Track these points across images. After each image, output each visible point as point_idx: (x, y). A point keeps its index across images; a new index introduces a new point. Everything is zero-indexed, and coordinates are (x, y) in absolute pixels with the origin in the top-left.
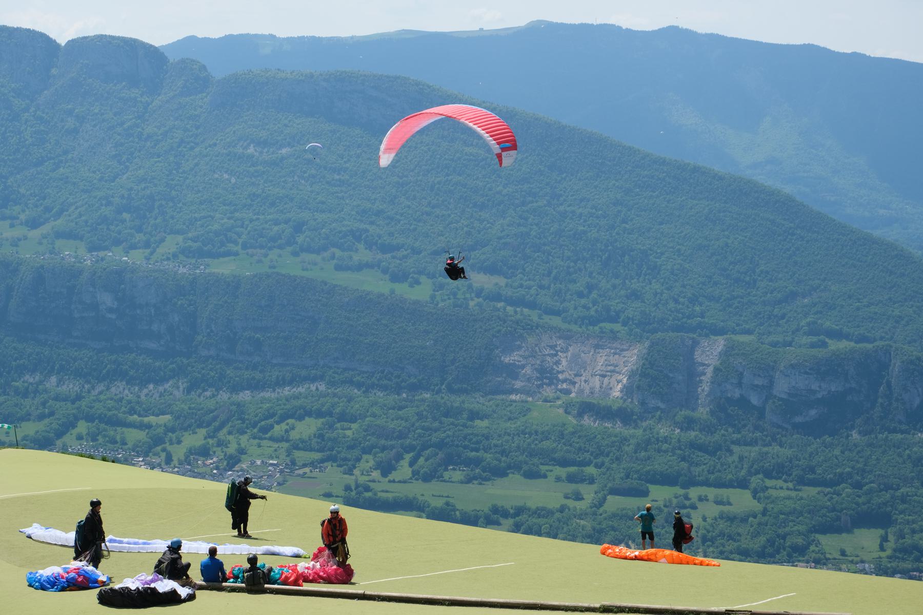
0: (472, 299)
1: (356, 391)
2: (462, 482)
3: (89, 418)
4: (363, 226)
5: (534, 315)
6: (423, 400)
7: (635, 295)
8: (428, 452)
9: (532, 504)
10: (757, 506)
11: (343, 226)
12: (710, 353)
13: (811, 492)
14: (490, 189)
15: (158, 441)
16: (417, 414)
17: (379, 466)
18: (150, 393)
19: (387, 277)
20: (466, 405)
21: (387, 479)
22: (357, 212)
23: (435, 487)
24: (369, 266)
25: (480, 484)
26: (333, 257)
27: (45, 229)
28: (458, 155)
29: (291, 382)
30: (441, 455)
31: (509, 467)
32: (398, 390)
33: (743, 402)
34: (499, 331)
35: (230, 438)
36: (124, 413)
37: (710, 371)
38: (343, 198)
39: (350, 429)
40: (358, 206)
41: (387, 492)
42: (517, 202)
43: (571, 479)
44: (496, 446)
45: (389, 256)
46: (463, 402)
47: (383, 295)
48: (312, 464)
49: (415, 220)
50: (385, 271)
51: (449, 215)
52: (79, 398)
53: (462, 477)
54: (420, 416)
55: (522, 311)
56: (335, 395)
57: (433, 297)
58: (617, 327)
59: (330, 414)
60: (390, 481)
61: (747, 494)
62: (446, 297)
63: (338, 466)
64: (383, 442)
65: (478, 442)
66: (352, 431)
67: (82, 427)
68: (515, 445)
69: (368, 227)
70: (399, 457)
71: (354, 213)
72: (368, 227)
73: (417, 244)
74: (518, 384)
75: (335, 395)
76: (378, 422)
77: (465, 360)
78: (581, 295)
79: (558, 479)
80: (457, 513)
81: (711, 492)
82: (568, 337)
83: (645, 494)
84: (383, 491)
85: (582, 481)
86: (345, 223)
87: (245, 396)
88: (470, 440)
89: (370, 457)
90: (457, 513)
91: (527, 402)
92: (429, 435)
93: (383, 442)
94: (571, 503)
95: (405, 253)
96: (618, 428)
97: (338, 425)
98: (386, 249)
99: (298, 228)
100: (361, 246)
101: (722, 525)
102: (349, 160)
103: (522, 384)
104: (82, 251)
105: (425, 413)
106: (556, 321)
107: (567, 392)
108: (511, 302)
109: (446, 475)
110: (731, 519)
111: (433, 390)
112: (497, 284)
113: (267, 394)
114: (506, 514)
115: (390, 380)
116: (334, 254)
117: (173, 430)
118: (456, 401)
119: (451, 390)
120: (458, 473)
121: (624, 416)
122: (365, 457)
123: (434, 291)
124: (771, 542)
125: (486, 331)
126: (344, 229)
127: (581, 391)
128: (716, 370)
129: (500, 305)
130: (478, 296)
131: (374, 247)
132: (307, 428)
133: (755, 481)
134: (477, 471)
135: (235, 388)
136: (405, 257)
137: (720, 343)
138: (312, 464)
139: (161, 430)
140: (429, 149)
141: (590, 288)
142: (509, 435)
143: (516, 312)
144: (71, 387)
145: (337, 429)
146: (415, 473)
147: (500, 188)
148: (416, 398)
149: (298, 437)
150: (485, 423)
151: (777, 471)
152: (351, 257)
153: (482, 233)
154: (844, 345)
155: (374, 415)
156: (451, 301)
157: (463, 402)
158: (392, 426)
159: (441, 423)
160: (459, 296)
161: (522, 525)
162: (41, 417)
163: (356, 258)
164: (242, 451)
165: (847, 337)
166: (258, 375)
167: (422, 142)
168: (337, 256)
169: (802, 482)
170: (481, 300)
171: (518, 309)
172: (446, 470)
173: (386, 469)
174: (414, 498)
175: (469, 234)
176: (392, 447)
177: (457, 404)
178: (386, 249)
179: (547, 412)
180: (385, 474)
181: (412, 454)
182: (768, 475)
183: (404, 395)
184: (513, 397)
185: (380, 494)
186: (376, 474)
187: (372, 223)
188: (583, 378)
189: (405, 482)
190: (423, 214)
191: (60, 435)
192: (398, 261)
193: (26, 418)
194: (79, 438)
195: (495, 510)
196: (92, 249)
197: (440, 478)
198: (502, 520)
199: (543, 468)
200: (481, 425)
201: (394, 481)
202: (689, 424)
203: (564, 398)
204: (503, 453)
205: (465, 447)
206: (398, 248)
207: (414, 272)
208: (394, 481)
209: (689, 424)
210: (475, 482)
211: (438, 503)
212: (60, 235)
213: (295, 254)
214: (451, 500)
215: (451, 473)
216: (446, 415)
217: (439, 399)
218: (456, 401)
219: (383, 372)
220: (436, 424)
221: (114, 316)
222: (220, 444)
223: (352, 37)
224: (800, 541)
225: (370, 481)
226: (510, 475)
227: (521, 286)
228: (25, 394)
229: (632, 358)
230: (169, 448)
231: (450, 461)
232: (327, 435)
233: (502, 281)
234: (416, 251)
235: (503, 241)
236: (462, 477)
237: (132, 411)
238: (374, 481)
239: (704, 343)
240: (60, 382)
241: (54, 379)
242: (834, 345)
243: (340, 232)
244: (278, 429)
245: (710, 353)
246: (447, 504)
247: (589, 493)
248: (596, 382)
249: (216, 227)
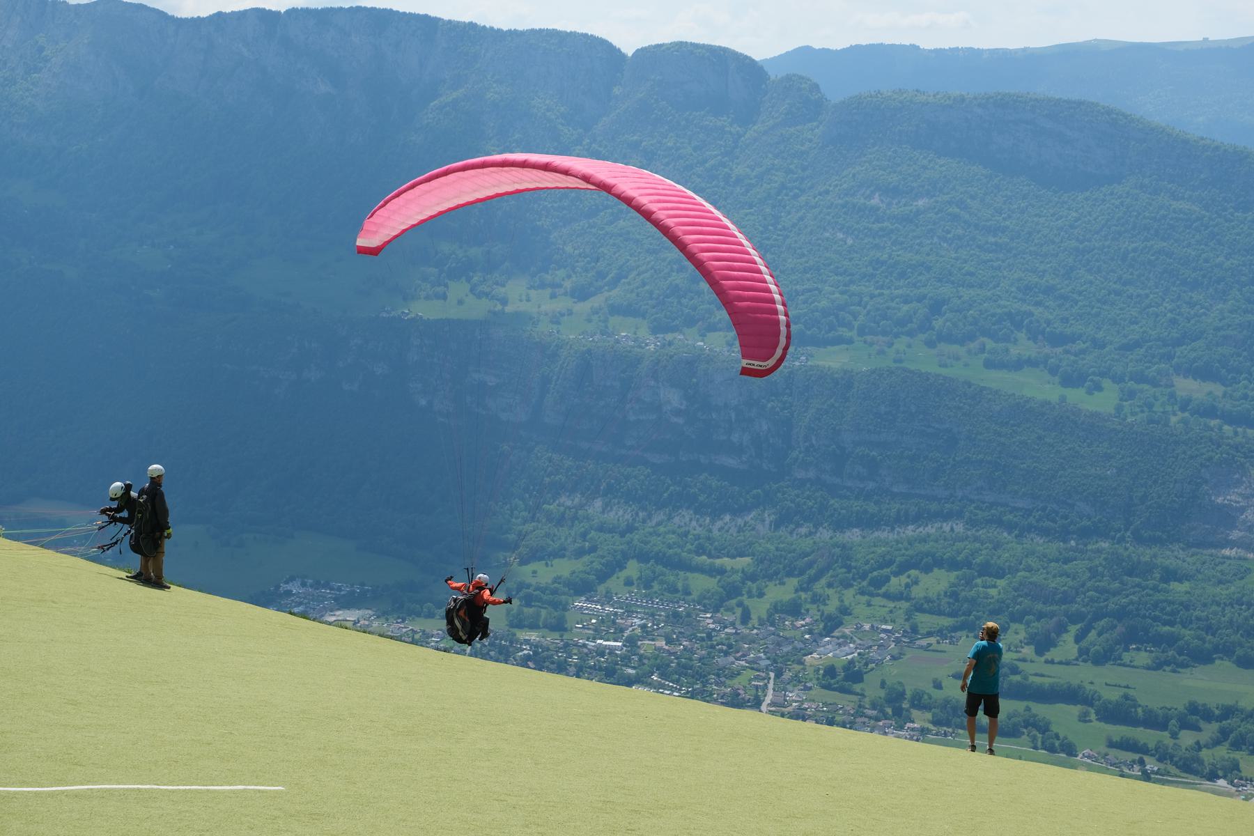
0: (1175, 414)
1: (1005, 534)
2: (1148, 668)
3: (643, 557)
4: (1026, 308)
6: (1099, 551)
8: (1102, 623)
11: (999, 306)
14: (1206, 261)
15: (732, 591)
16: (1090, 569)
17: (1031, 640)
18: (725, 527)
19: (1057, 379)
20: (1159, 561)
21: (1043, 659)
22: (1018, 288)
24: (1032, 363)
25: (1174, 671)
26: (982, 349)
27: (596, 301)
28: (1162, 212)
29: (920, 518)
30: (1120, 629)
31: (1216, 649)
32: (1064, 535)
34: (1210, 459)
35: (830, 592)
36: (689, 552)
38: (999, 268)
39: (995, 586)
40: (1020, 279)
41: (1043, 676)
42: (1244, 279)
44: (1198, 619)
45: (1060, 350)
46: (1155, 556)
47: (1049, 403)
48: (941, 633)
49: (1098, 301)
50: (1053, 371)
51: (1147, 296)
52: (630, 529)
53: (1149, 662)
54: (1094, 572)
55: (1245, 432)
56: (976, 539)
57: (1119, 409)
59: (968, 564)
60: (1047, 662)
62: (1138, 410)
64: (1039, 606)
65: (1173, 613)
66: (998, 589)
67: (633, 569)
68: (1226, 619)
69: (1032, 308)
70: (1061, 629)
71: (1013, 289)
72: (1032, 308)
73: (1100, 335)
74: (1235, 535)
75: (976, 539)
76: (1034, 579)
77: (1160, 497)
80: (1140, 710)
84: (1036, 675)
86: (1002, 303)
87: (853, 536)
88: (1164, 609)
89: (1021, 627)
90: (1140, 710)
91: (1245, 559)
92: (1106, 600)
93: (1039, 606)
95: (1083, 346)
97: (979, 581)
98: (1058, 340)
99: (937, 307)
100: (1022, 335)
102: (1010, 217)
103: (1241, 534)
104: (644, 333)
105: (1100, 569)
108: (1230, 419)
109: (1126, 657)
111: (1113, 538)
112: (1210, 393)
113: (883, 534)
114: (1208, 716)
115: (1054, 521)
116: (984, 345)
117: (753, 578)
118: (1145, 554)
119: (1139, 539)
120: (1144, 654)
122: (1014, 626)
123: (1121, 400)
125: (1191, 457)
126: (999, 311)
129: (1214, 423)
130: (1183, 409)
131: (1040, 337)
132: (935, 583)
134: (1170, 653)
135: (840, 525)
136: (1083, 352)
138: (941, 633)
139: (737, 577)
140: (1122, 204)
142: (1218, 604)
143: (1236, 433)
144: (620, 514)
145: (976, 585)
146: (1083, 653)
147: (1221, 259)
148: (1089, 547)
149: (922, 595)
150: (1185, 586)
152: (1007, 350)
153: (1192, 322)
155: (1029, 569)
156: (1145, 415)
157: (1155, 556)
158: (1053, 585)
159: (1122, 583)
160: (1158, 408)
161: (1231, 732)
162: (580, 553)
163: (1014, 351)
164: (845, 611)
166: (872, 508)
167: (1112, 194)
168: (988, 347)
170: (1187, 414)
171: (1239, 429)
172: (1127, 650)
174: (1080, 687)
175: (1173, 322)
176: (1052, 615)
177: (1147, 558)
178: (1058, 340)
180: (1040, 651)
181: (1078, 626)
183: (1073, 543)
184: (1227, 552)
185: (1032, 679)
186: (1028, 651)
187: (1038, 304)
189: (1068, 663)
190: (1110, 294)
191: (603, 576)
192: (1072, 358)
193: (560, 553)
194: (629, 582)
195: (1193, 709)
196: (656, 329)
197: (1118, 661)
198: (1202, 724)
200: (1179, 589)
201: (1052, 662)
204: (1209, 629)
205: (1155, 619)
206: (1073, 339)
207: (1094, 374)
208: (1052, 662)
210: (1168, 669)
211: (1113, 695)
212: (615, 310)
213: (930, 344)
214: (1131, 692)
215: (1133, 654)
217: (1121, 551)
218: (1145, 554)
219: (1044, 509)
220: (1117, 585)
221: (680, 421)
222: (816, 599)
223: (1025, 50)
225: (1019, 660)
226: (1218, 662)
227: (1245, 397)
228: (560, 521)
230: (747, 602)
231: (1134, 637)
232: (963, 594)
233: (1218, 389)
234: (1098, 345)
235: (1222, 333)
236: (1149, 662)
237: (700, 550)
238: (1024, 660)
240: (606, 507)
241: (598, 503)
243: (993, 315)
244: (896, 583)
246: (1126, 697)
249: (824, 303)
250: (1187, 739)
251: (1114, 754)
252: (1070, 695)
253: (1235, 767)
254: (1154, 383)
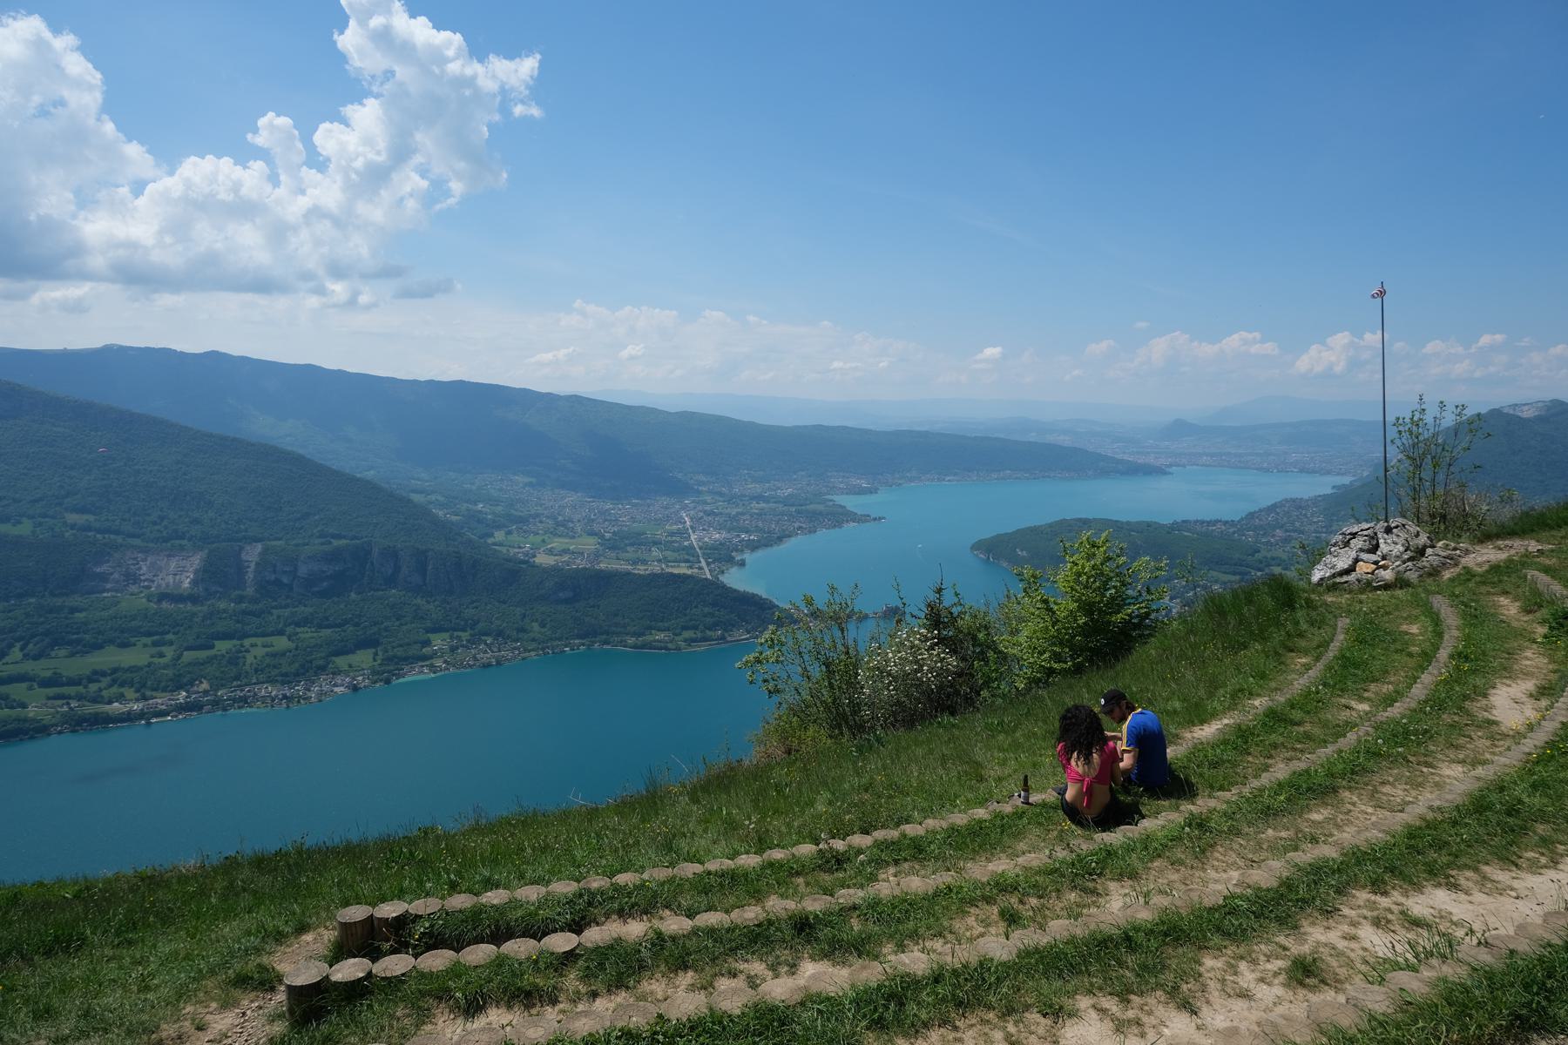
5: (119, 539)
7: (196, 521)
9: (125, 665)
10: (291, 645)
12: (252, 554)
13: (326, 632)
23: (43, 663)
33: (278, 582)
37: (253, 565)
43: (155, 644)
58: (184, 542)
61: (284, 639)
70: (11, 646)
74: (109, 586)
78: (155, 523)
79: (145, 645)
81: (259, 641)
82: (146, 551)
83: (212, 647)
85: (164, 644)
94: (156, 660)
96: (189, 607)
101: (268, 660)
106: (137, 542)
107: (148, 587)
108: (99, 531)
110: (274, 655)
114: (104, 674)
118: (59, 601)
121: (193, 599)
124: (302, 666)
127: (159, 586)
128: (257, 564)
133: (289, 630)
137: (259, 547)
141: (162, 518)
150: (82, 615)
151: (305, 622)
154: (343, 542)
165: (344, 537)
169: (320, 626)
179: (134, 601)
182: (298, 625)
195: (95, 672)
197: (48, 656)
202: (240, 599)
203: (146, 592)
209: (240, 599)
211: (48, 674)
216: (51, 611)
218: (59, 601)
224: (321, 662)
229: (197, 560)
231: (55, 643)
233: (91, 518)
239: (248, 548)
242: (336, 543)
245: (252, 554)
247: (169, 652)
248: (170, 579)
250: (93, 687)
251: (50, 702)
252: (21, 678)
253: (122, 695)
254: (53, 517)
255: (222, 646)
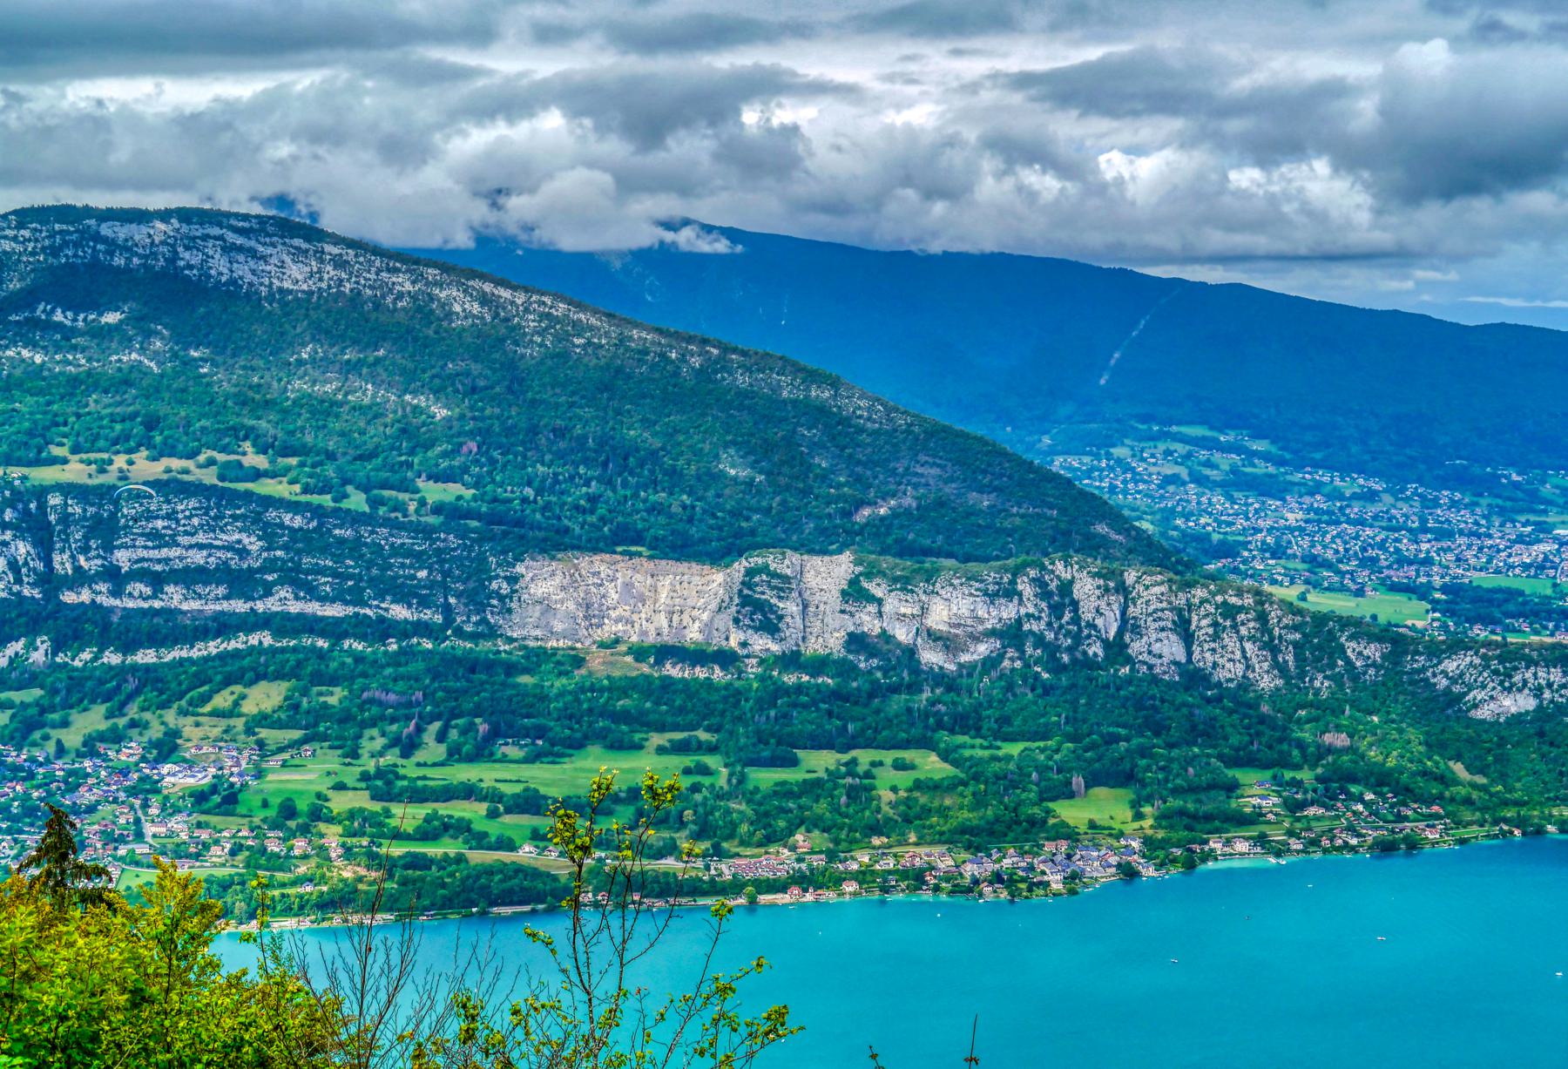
35: (147, 716)
63: (331, 747)
139: (33, 711)
149: (255, 711)
173: (409, 747)
180: (406, 755)
188: (643, 616)
199: (637, 737)
255: (819, 762)
